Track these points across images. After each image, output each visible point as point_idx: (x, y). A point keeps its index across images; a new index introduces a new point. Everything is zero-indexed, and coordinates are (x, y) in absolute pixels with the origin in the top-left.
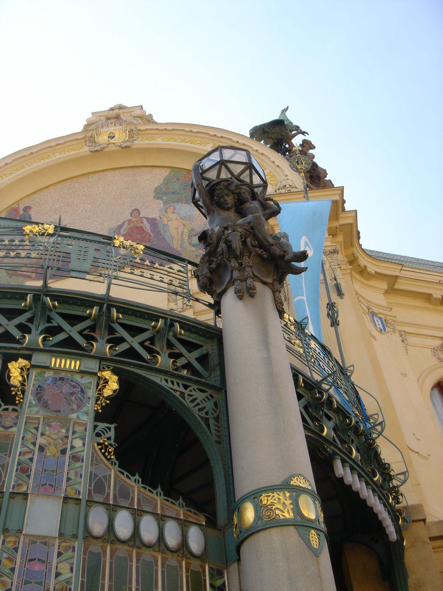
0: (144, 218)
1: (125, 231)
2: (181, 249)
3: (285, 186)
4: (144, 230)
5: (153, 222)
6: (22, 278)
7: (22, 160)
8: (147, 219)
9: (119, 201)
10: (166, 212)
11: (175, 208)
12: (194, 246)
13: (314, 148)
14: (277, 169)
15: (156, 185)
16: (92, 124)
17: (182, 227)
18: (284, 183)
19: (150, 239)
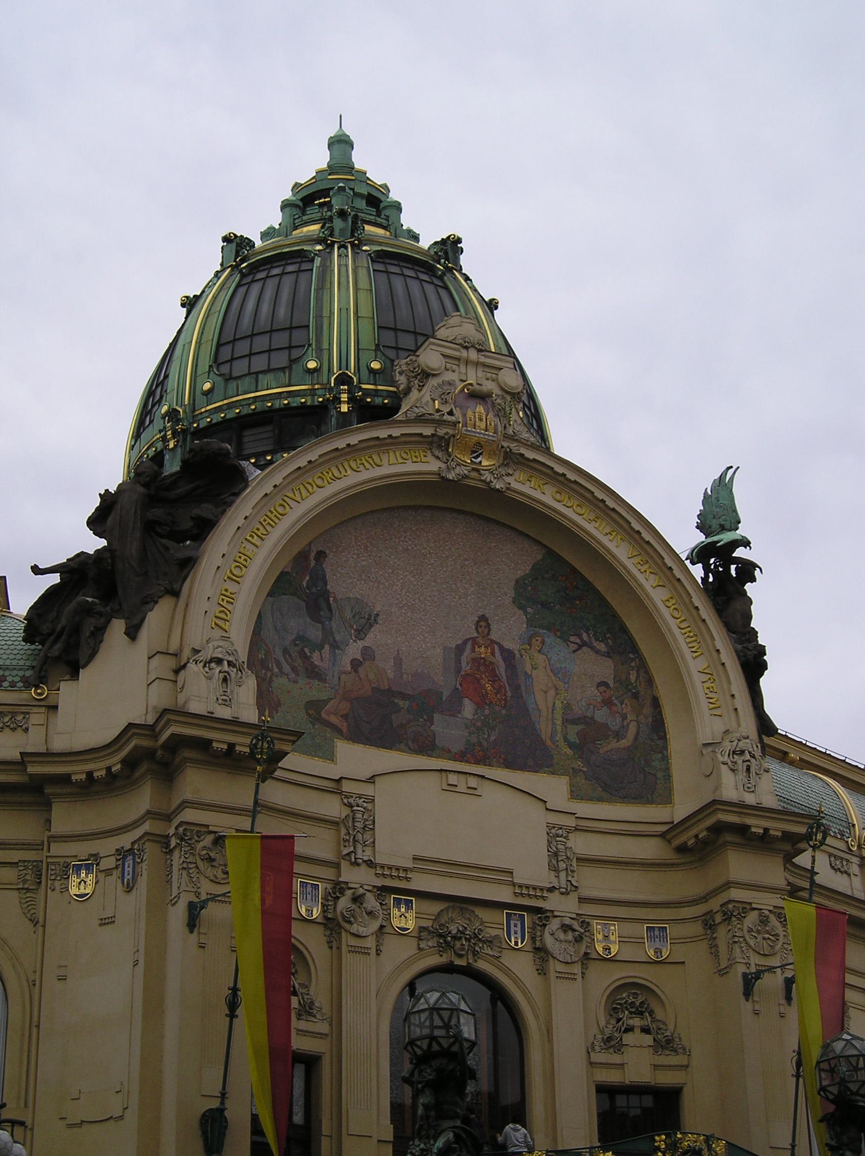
0: (497, 643)
1: (468, 664)
2: (553, 747)
3: (742, 752)
4: (496, 676)
5: (508, 656)
6: (329, 730)
7: (332, 455)
8: (501, 647)
9: (459, 585)
10: (530, 645)
11: (543, 642)
12: (571, 745)
13: (753, 579)
14: (720, 668)
15: (520, 573)
16: (434, 375)
17: (552, 692)
18: (742, 745)
19: (506, 700)
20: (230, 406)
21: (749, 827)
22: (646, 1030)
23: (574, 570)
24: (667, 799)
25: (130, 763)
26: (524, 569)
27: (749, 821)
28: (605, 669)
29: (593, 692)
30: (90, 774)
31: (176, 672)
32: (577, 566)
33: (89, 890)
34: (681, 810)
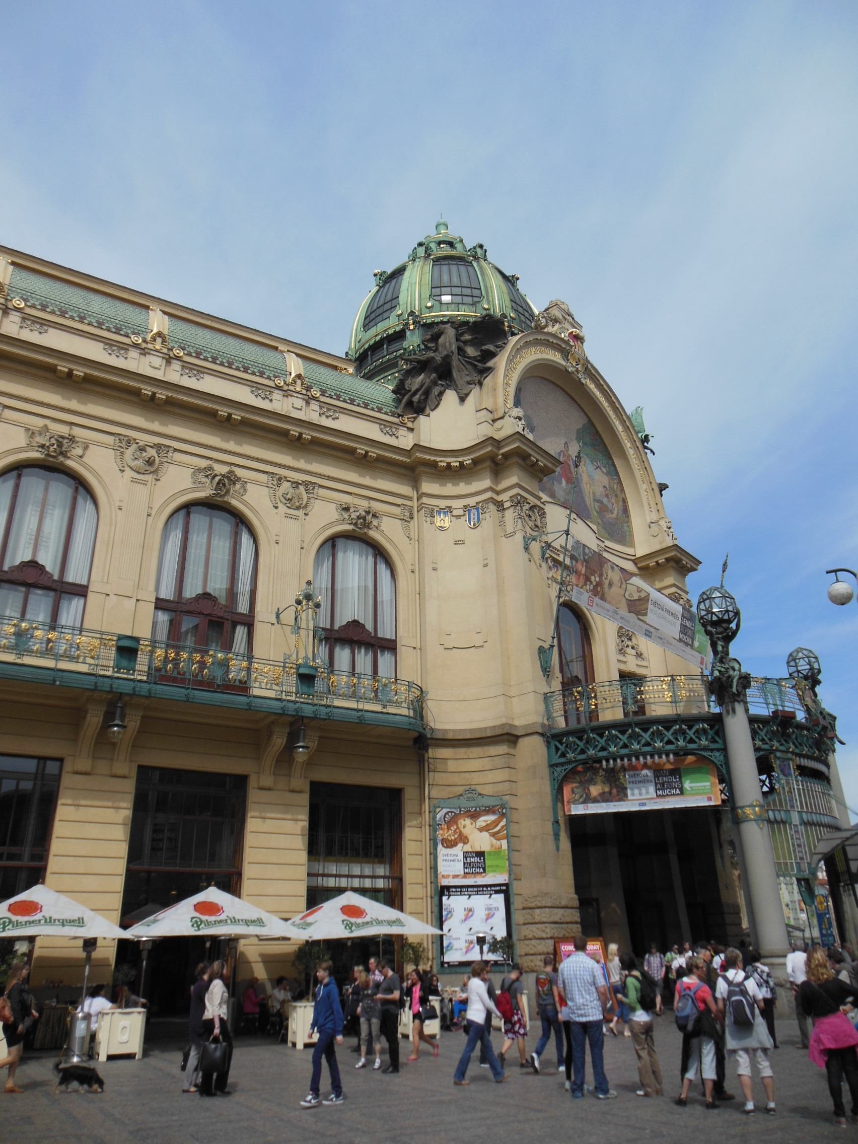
20: (444, 316)
21: (682, 560)
22: (633, 648)
23: (597, 432)
24: (632, 544)
25: (476, 462)
26: (580, 426)
27: (683, 558)
28: (605, 480)
29: (602, 489)
30: (449, 464)
31: (494, 421)
32: (599, 429)
33: (447, 525)
34: (641, 550)
